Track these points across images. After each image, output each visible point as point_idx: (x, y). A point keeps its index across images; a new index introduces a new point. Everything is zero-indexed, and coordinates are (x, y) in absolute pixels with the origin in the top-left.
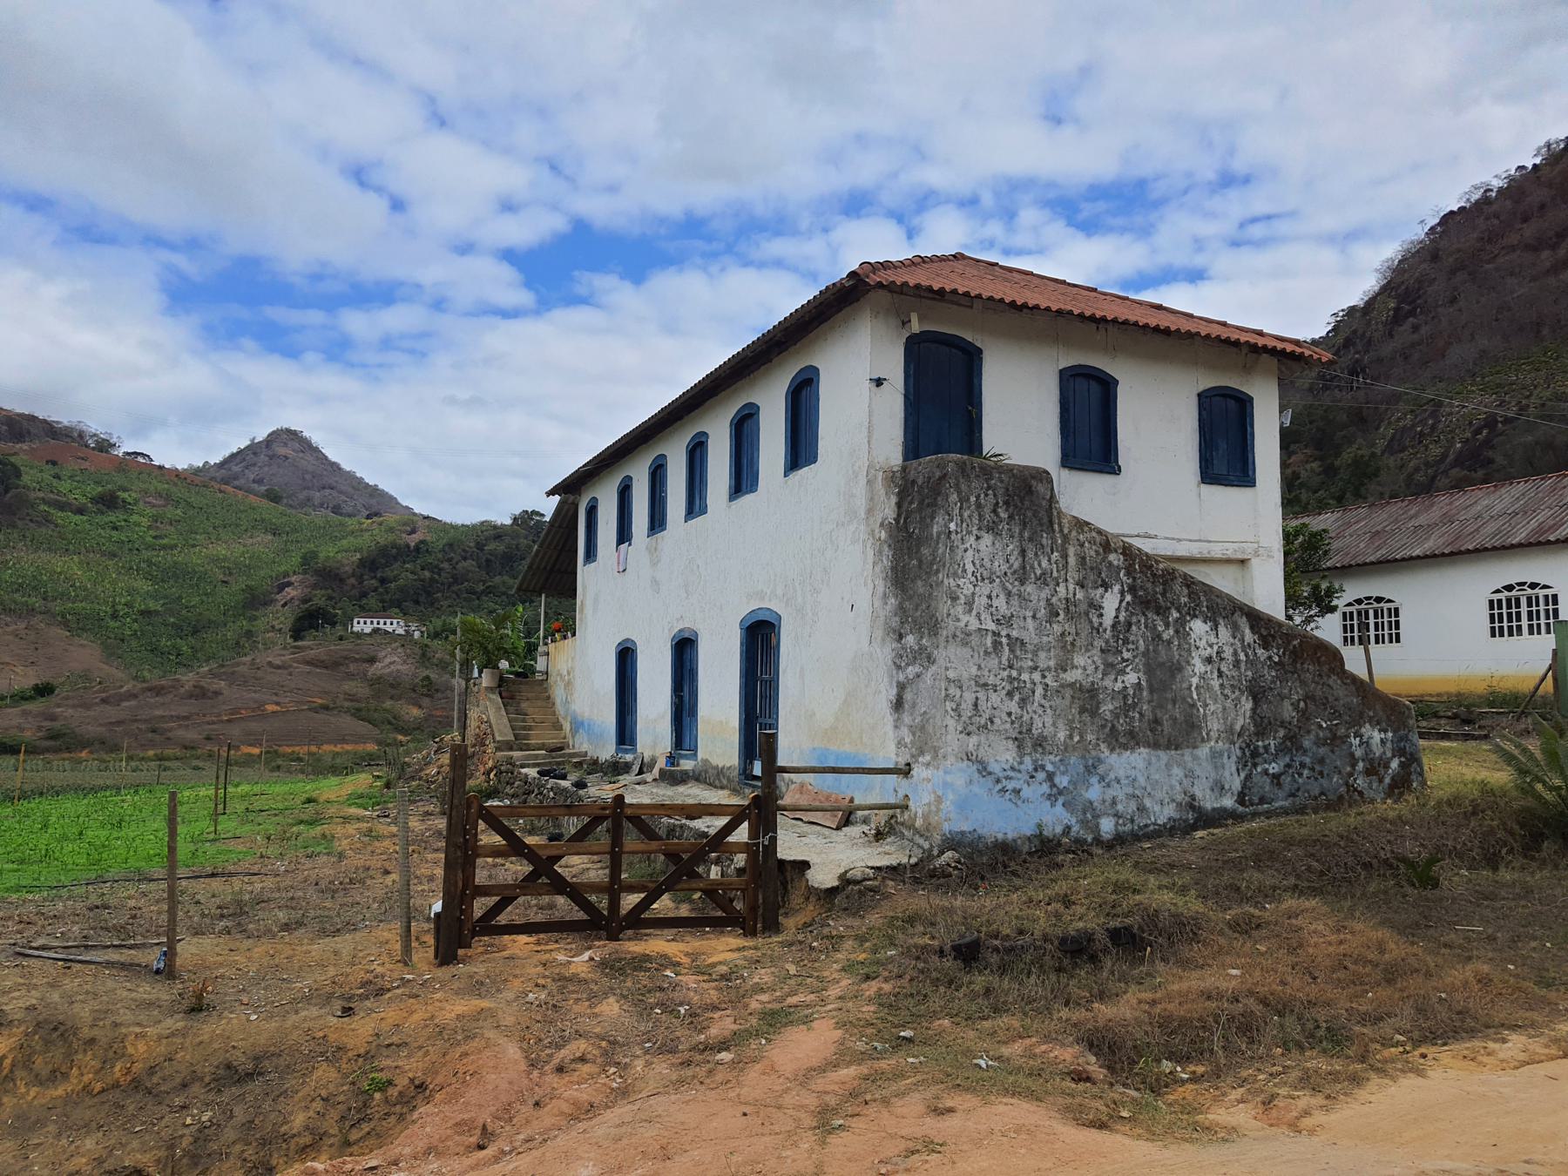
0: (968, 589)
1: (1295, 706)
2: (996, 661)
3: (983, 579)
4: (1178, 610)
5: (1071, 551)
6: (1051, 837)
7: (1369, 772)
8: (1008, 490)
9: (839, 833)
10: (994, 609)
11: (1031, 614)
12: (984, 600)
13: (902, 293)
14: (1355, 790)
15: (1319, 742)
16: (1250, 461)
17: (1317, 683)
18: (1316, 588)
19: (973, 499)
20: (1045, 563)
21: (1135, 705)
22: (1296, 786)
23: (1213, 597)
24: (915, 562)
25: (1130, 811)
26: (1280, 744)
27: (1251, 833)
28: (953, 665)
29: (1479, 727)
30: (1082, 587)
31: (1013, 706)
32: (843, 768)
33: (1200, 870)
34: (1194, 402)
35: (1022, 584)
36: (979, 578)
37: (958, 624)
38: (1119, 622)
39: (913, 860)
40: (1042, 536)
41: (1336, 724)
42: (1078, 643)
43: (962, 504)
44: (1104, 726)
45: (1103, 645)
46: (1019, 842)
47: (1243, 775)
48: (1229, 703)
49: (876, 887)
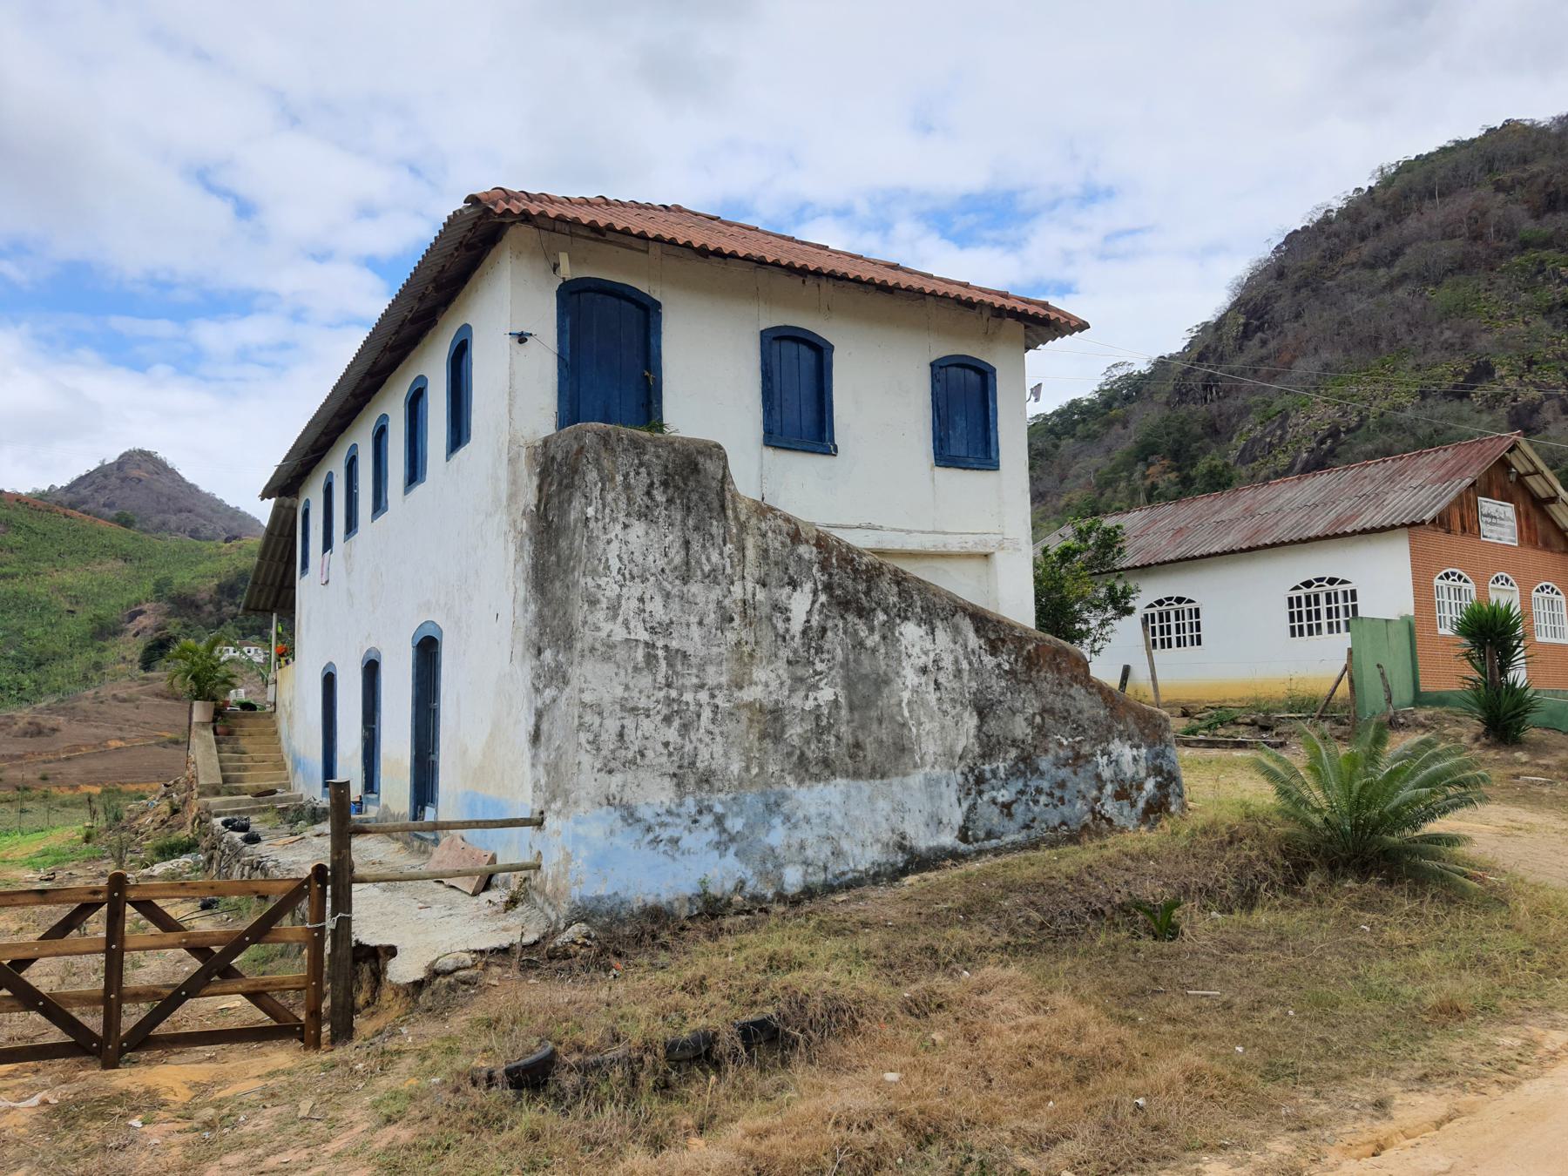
0: (612, 590)
1: (1030, 722)
2: (650, 678)
3: (633, 578)
4: (886, 611)
5: (750, 543)
6: (719, 896)
7: (1120, 795)
8: (666, 467)
9: (475, 900)
10: (646, 615)
11: (697, 619)
12: (634, 604)
13: (554, 231)
14: (1103, 817)
15: (1059, 763)
16: (993, 440)
17: (1057, 694)
18: (1112, 589)
19: (619, 478)
20: (715, 557)
21: (830, 726)
22: (1030, 816)
23: (929, 596)
24: (553, 558)
25: (822, 856)
26: (1012, 767)
27: (967, 877)
28: (591, 686)
29: (1277, 734)
30: (764, 585)
31: (672, 734)
32: (449, 823)
33: (898, 928)
34: (928, 370)
35: (685, 581)
36: (628, 576)
37: (597, 634)
38: (810, 628)
39: (529, 939)
40: (711, 524)
41: (1079, 742)
42: (758, 654)
43: (604, 485)
44: (789, 755)
45: (791, 655)
46: (676, 905)
47: (965, 805)
48: (949, 721)
49: (472, 977)
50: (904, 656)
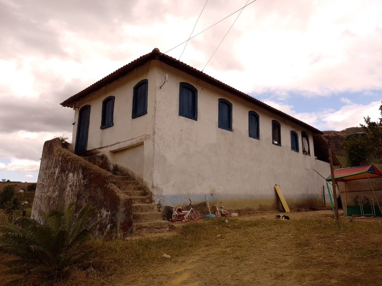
16: (146, 103)
35: (46, 170)
50: (68, 183)
